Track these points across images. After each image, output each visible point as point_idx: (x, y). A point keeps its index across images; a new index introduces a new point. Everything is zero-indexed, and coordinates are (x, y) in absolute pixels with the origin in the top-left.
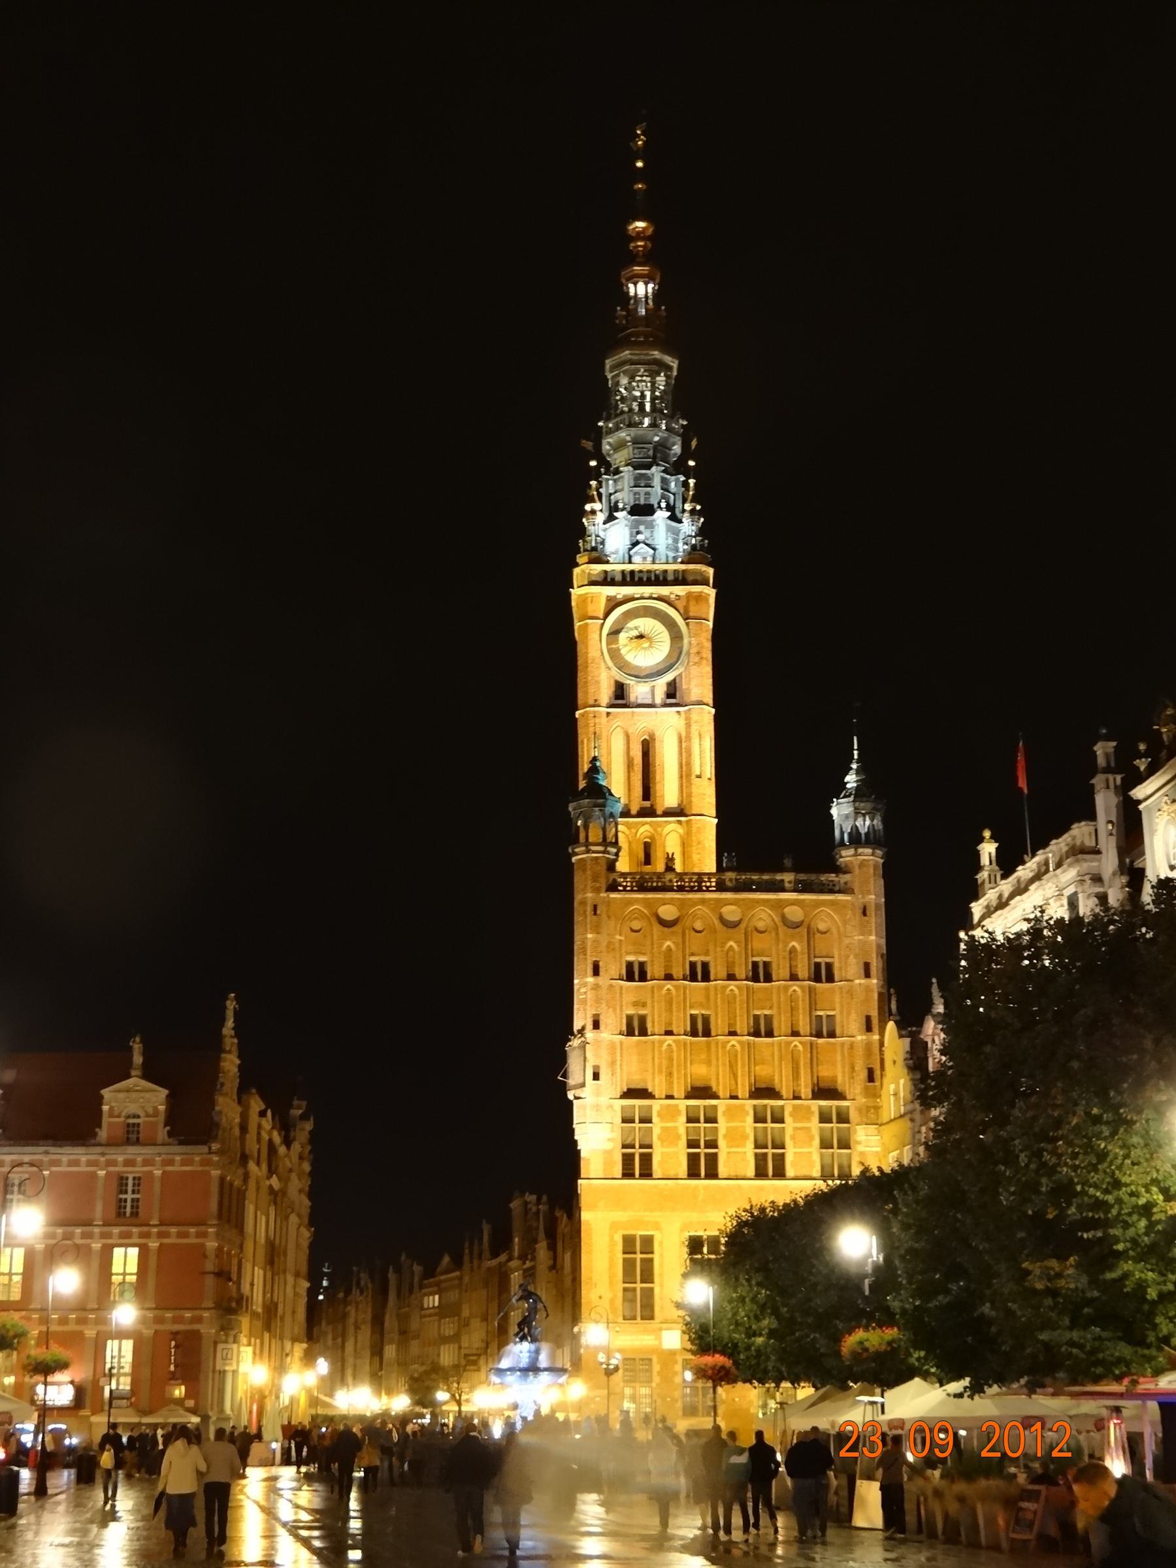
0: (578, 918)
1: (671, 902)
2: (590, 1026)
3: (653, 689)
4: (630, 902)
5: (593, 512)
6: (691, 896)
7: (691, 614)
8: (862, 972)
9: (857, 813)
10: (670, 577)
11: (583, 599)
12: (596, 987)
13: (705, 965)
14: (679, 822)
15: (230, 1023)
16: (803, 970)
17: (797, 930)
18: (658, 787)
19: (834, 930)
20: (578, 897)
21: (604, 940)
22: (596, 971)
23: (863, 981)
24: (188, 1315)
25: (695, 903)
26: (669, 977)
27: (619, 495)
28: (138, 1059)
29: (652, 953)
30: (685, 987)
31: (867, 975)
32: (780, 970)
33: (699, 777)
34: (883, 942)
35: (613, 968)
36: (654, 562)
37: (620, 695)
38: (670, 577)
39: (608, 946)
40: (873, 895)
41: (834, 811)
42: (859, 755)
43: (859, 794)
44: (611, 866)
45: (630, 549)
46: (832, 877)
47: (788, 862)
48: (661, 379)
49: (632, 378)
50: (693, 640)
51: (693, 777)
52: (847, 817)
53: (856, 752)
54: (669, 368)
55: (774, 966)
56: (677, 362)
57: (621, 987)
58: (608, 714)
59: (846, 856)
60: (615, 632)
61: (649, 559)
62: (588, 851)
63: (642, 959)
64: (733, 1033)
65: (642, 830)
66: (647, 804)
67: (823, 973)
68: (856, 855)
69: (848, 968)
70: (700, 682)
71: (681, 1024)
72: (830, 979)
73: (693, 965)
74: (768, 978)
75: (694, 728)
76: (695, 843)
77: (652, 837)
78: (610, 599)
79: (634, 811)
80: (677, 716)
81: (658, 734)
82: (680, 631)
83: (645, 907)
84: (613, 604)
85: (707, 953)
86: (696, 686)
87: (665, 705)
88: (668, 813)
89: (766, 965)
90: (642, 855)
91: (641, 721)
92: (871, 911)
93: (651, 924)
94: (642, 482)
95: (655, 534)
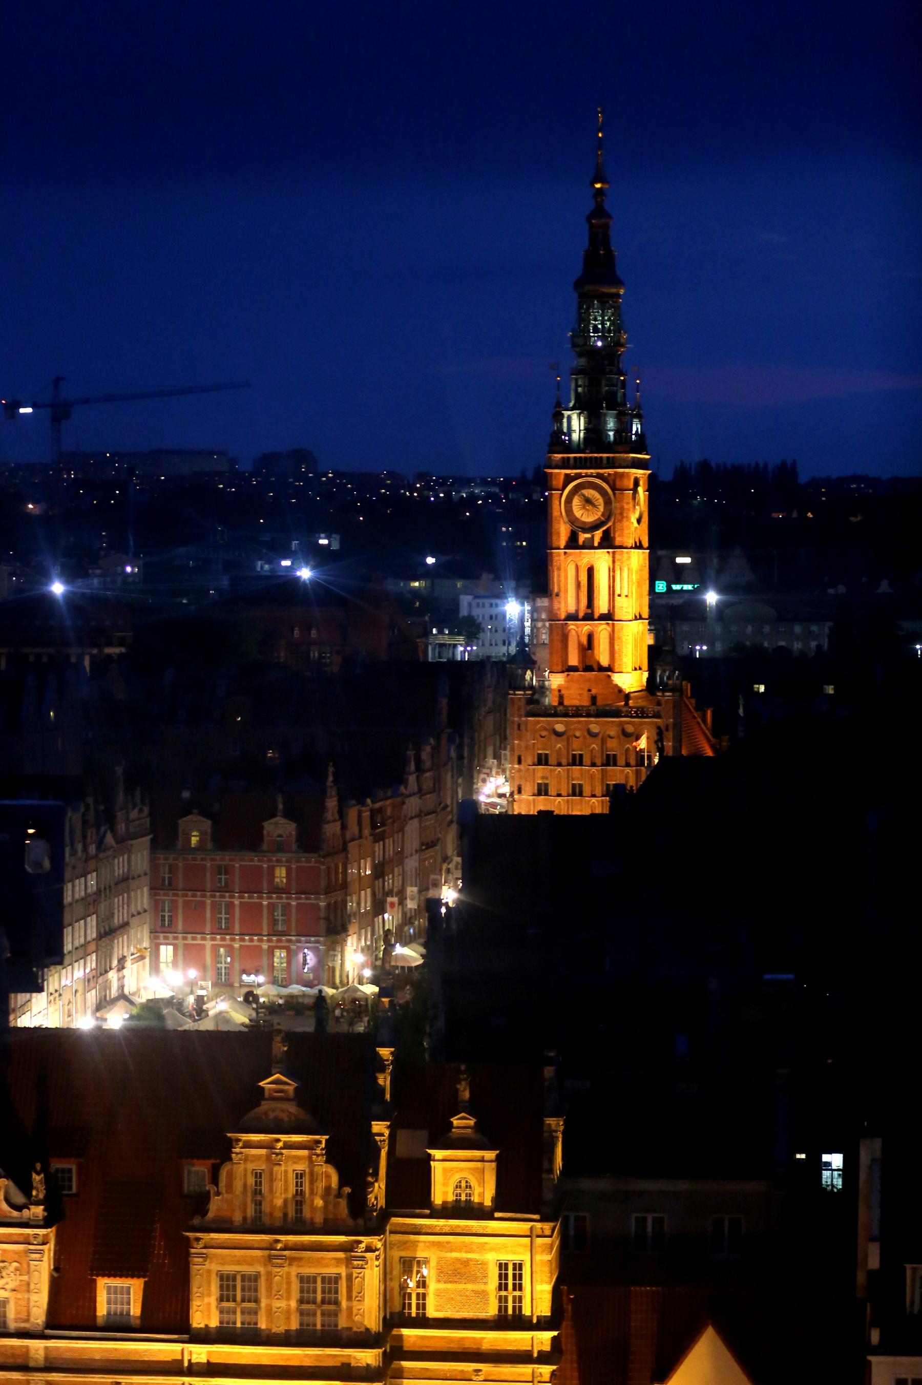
2: (516, 792)
12: (519, 770)
15: (331, 779)
24: (313, 939)
26: (559, 765)
28: (281, 806)
33: (619, 595)
35: (529, 759)
37: (573, 543)
51: (616, 595)
55: (618, 758)
64: (593, 796)
65: (585, 628)
66: (589, 611)
71: (565, 789)
75: (617, 563)
78: (567, 475)
82: (610, 498)
89: (615, 756)
91: (588, 557)
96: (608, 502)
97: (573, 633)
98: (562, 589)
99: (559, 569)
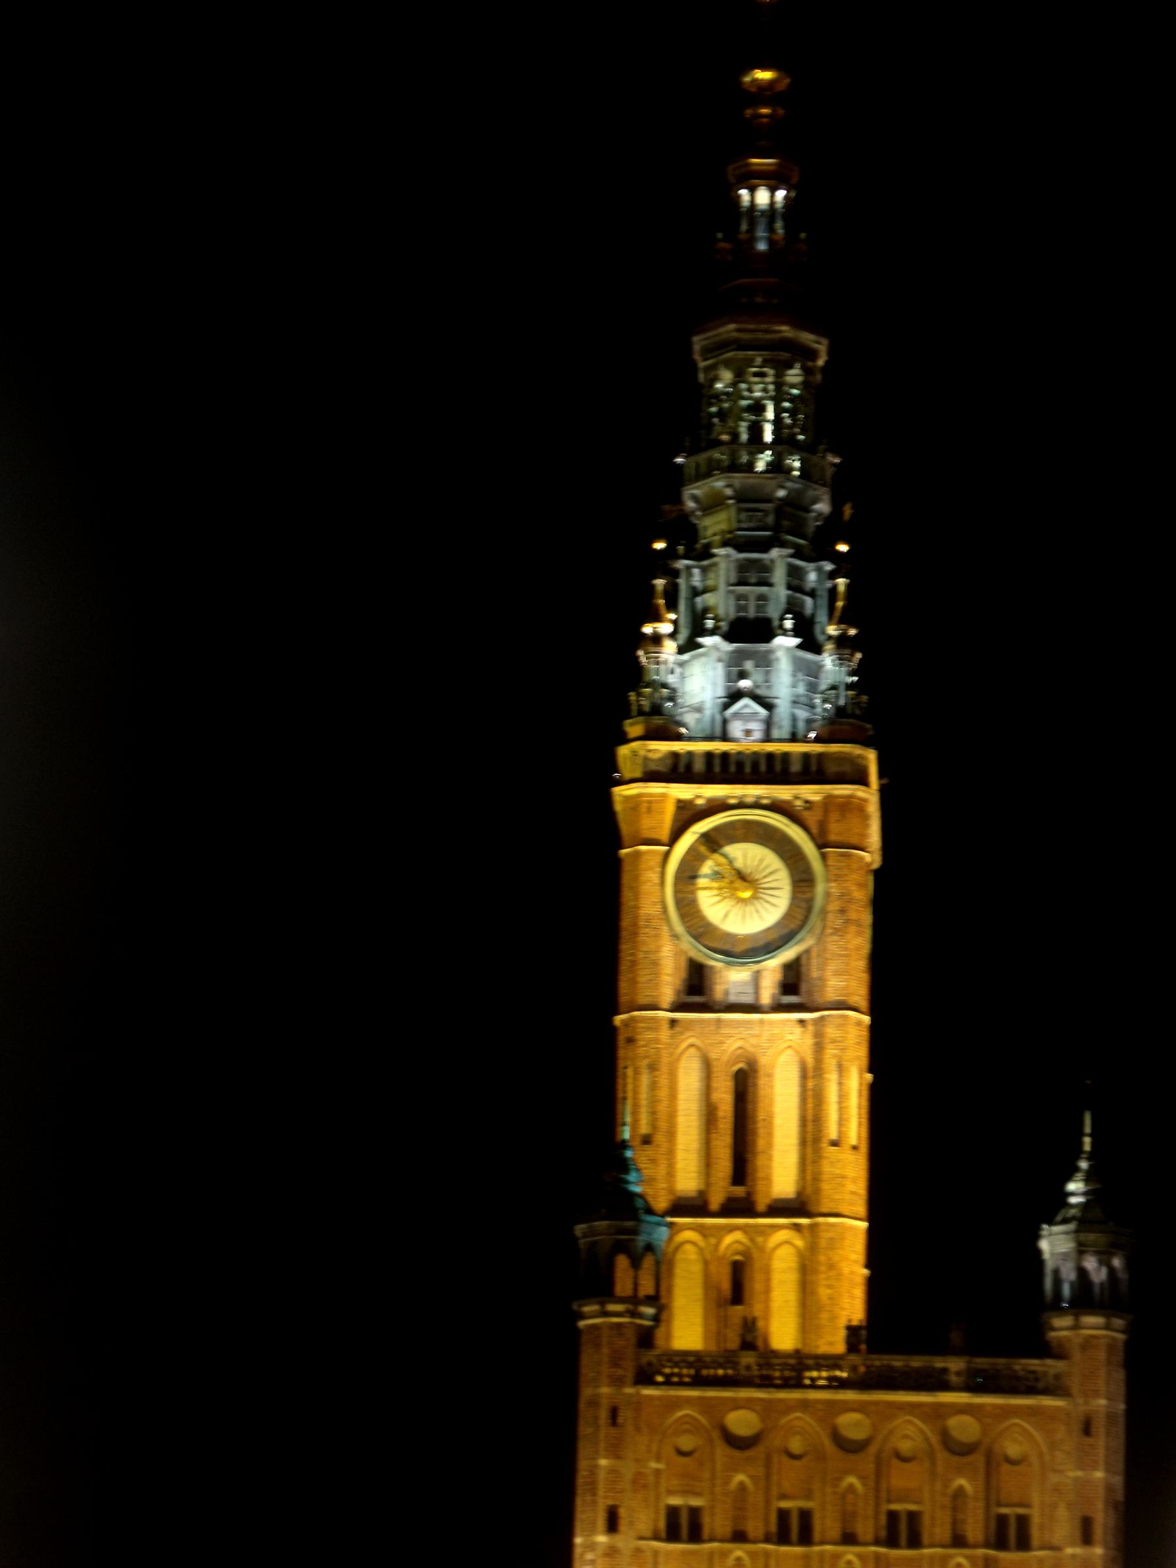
0: (584, 1429)
1: (748, 1404)
3: (757, 976)
4: (677, 1403)
5: (657, 639)
6: (783, 1395)
7: (833, 837)
8: (1078, 1533)
9: (1081, 1250)
10: (796, 767)
11: (634, 803)
12: (611, 1552)
13: (806, 1517)
14: (797, 1228)
16: (974, 1529)
17: (970, 1458)
18: (760, 1161)
19: (1034, 1460)
20: (586, 1392)
21: (628, 1469)
22: (612, 1525)
23: (1078, 1551)
25: (789, 1407)
26: (739, 1537)
27: (709, 599)
29: (713, 1493)
30: (767, 1554)
31: (1087, 1539)
32: (937, 1526)
33: (835, 1144)
34: (1118, 1480)
35: (642, 1517)
36: (768, 738)
38: (796, 767)
39: (634, 1482)
40: (1104, 1399)
41: (1044, 1245)
42: (1093, 1144)
43: (1085, 1220)
44: (646, 1339)
45: (726, 706)
46: (1034, 1364)
47: (956, 1337)
48: (794, 375)
49: (740, 376)
50: (834, 889)
51: (824, 1145)
52: (1065, 1257)
53: (1087, 1142)
54: (810, 354)
55: (926, 1520)
56: (825, 342)
57: (656, 1553)
58: (673, 1022)
59: (1061, 1326)
60: (688, 874)
61: (757, 727)
62: (606, 1314)
63: (695, 1502)
65: (729, 1239)
66: (740, 1191)
67: (1011, 1533)
68: (1076, 1327)
69: (1055, 1525)
70: (844, 969)
72: (1024, 1544)
73: (783, 1515)
74: (915, 1541)
75: (830, 1052)
76: (816, 1280)
77: (747, 1254)
78: (682, 805)
79: (716, 1201)
80: (798, 1030)
81: (763, 1060)
83: (702, 1413)
84: (688, 815)
85: (808, 1496)
86: (837, 973)
87: (778, 1008)
88: (780, 1209)
89: (913, 1517)
90: (726, 1286)
91: (736, 1036)
92: (1099, 1427)
93: (711, 1441)
94: (752, 574)
95: (774, 679)
96: (802, 879)
97: (690, 1252)
98: (663, 1125)
99: (653, 1068)
